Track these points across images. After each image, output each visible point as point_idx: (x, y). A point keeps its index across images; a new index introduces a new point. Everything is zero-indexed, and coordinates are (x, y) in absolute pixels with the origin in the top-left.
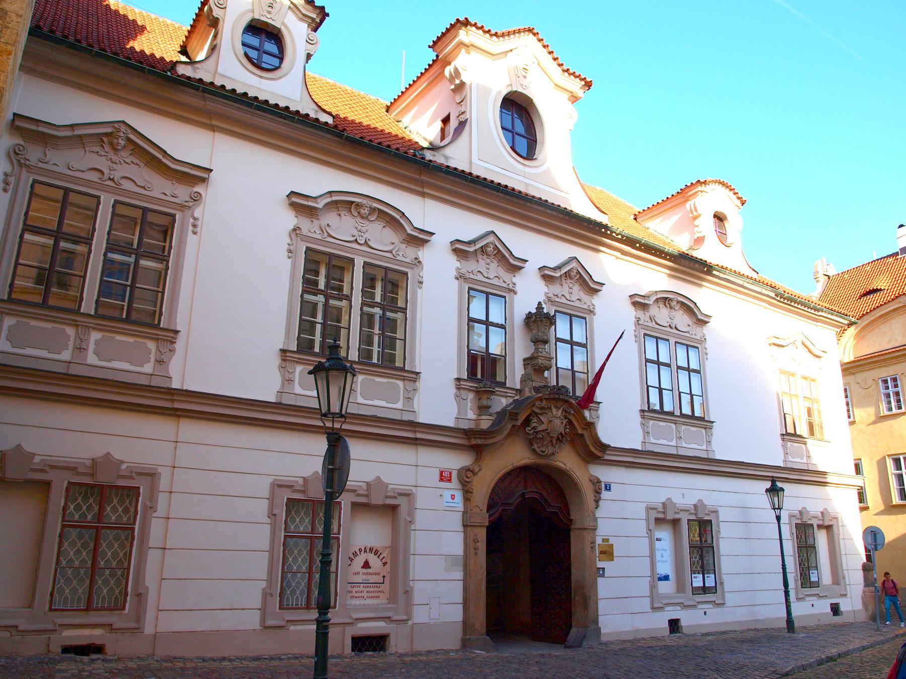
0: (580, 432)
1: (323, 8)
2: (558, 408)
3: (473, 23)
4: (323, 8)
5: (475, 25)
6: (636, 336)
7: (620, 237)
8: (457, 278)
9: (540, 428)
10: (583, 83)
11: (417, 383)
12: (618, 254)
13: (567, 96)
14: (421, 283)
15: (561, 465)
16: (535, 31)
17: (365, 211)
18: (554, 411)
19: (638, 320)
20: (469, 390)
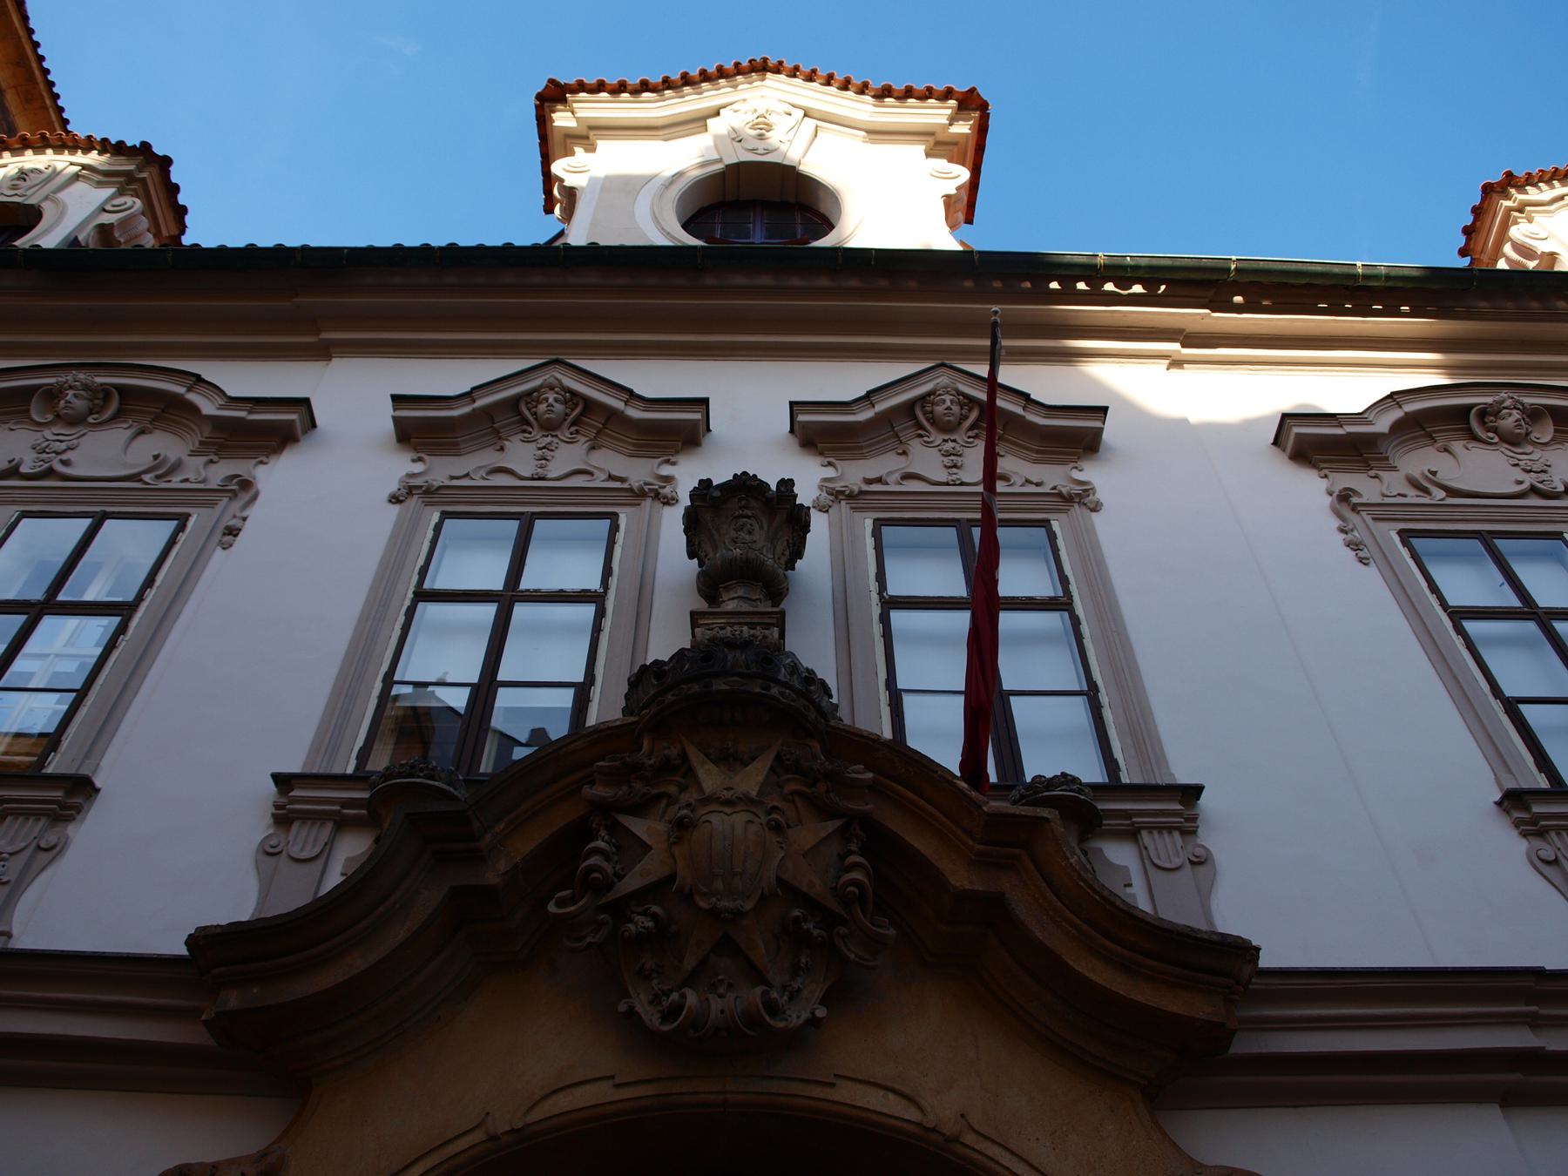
0: (961, 878)
1: (146, 146)
2: (729, 760)
3: (572, 81)
4: (146, 146)
5: (581, 87)
6: (1355, 546)
7: (1137, 289)
8: (395, 499)
9: (632, 882)
10: (953, 103)
11: (71, 829)
12: (1174, 347)
13: (920, 149)
14: (233, 532)
15: (871, 1100)
16: (773, 61)
17: (75, 401)
18: (711, 778)
19: (1344, 497)
20: (342, 824)
